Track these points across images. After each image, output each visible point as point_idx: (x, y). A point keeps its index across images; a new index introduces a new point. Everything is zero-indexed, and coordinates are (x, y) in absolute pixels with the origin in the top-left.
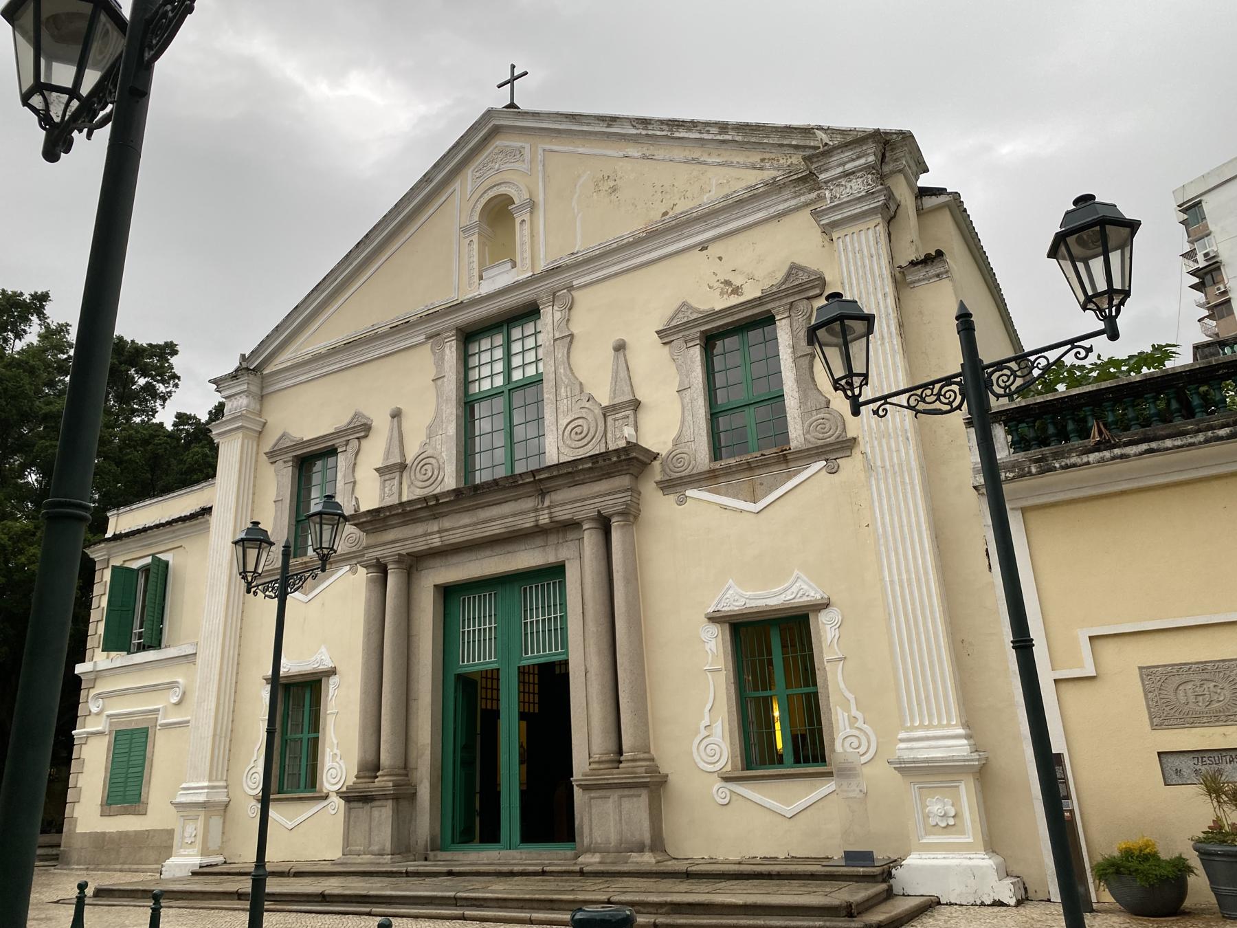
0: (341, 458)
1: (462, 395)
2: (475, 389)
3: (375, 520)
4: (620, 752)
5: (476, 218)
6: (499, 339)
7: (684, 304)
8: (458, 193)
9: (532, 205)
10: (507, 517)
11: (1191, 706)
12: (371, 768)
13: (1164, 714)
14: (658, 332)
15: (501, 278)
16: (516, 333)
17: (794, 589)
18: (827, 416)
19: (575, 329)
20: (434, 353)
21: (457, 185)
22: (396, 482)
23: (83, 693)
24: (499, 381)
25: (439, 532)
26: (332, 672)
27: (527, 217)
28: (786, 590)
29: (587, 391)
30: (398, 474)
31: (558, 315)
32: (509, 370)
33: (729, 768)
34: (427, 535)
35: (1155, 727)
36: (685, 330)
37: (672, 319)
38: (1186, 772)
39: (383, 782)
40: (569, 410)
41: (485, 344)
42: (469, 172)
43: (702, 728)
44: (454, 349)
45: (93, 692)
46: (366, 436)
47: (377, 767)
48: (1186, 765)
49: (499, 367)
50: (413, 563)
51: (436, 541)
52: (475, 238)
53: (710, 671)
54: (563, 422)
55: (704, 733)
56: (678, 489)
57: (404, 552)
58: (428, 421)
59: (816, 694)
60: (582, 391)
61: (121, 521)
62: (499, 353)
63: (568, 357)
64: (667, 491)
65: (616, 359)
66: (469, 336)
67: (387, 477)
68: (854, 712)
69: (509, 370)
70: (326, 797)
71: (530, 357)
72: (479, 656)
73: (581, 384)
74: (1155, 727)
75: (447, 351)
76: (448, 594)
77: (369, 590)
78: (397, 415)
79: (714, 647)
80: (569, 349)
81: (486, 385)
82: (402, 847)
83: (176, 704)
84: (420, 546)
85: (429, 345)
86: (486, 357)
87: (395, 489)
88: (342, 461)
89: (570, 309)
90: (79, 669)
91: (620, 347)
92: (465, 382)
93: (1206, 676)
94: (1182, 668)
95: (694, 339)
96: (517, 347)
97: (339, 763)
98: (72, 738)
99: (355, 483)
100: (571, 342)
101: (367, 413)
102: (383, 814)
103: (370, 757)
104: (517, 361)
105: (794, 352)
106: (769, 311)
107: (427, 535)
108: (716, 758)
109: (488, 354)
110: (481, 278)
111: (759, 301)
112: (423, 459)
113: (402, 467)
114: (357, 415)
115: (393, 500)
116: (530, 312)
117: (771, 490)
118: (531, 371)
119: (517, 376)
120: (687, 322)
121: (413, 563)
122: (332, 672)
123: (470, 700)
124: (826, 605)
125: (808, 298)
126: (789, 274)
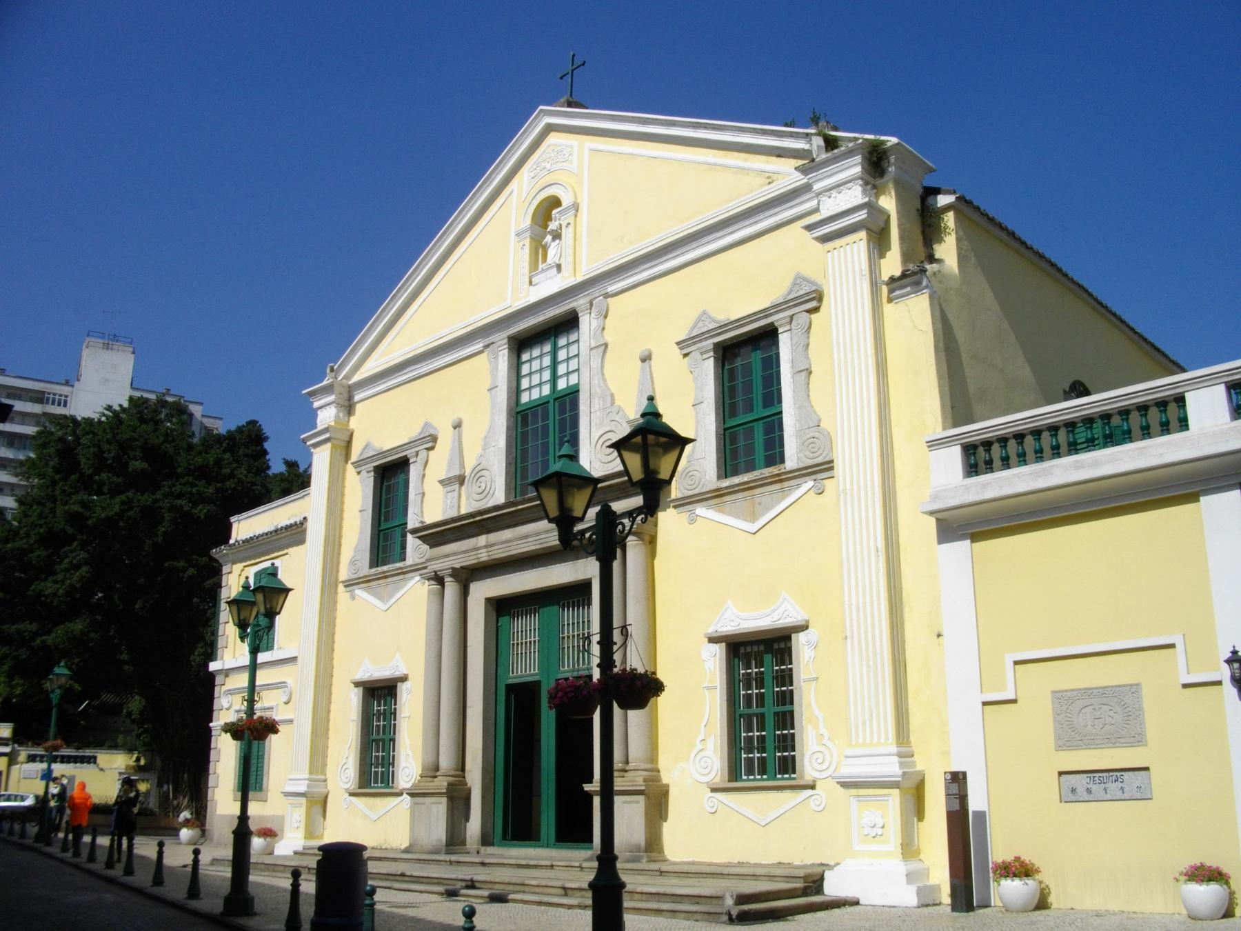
0: (412, 468)
1: (513, 405)
2: (525, 398)
3: (437, 535)
4: (627, 762)
5: (528, 222)
6: (547, 348)
7: (704, 313)
8: (514, 195)
9: (576, 207)
10: (541, 533)
11: (1089, 727)
12: (432, 770)
13: (1068, 738)
14: (678, 344)
15: (549, 285)
16: (562, 341)
17: (780, 611)
18: (816, 435)
19: (608, 337)
20: (490, 362)
21: (514, 185)
22: (456, 494)
23: (217, 689)
24: (546, 390)
25: (486, 547)
26: (404, 679)
27: (571, 220)
28: (774, 611)
29: (617, 403)
30: (456, 486)
31: (594, 323)
32: (554, 378)
33: (717, 780)
34: (483, 547)
35: (1059, 748)
36: (700, 341)
37: (694, 327)
38: (1081, 791)
39: (441, 783)
40: (602, 423)
41: (536, 352)
42: (525, 171)
43: (698, 741)
44: (506, 358)
45: (224, 688)
46: (432, 448)
47: (437, 768)
48: (1080, 782)
49: (547, 375)
50: (467, 576)
51: (484, 556)
52: (527, 242)
53: (708, 688)
54: (596, 435)
55: (699, 746)
56: (690, 507)
57: (457, 566)
58: (484, 434)
59: (792, 713)
60: (613, 403)
61: (245, 527)
62: (547, 361)
63: (602, 367)
64: (681, 509)
65: (643, 369)
66: (520, 344)
67: (449, 489)
68: (823, 730)
69: (554, 378)
70: (401, 794)
71: (573, 365)
72: (525, 668)
73: (612, 395)
74: (1059, 748)
75: (500, 360)
76: (501, 607)
77: (429, 602)
78: (458, 426)
79: (714, 660)
80: (603, 358)
81: (535, 394)
82: (455, 840)
83: (286, 703)
84: (470, 560)
85: (486, 353)
86: (536, 365)
87: (455, 500)
88: (414, 471)
89: (606, 317)
90: (213, 666)
91: (646, 359)
92: (516, 391)
93: (1105, 700)
94: (1087, 692)
95: (708, 351)
96: (562, 355)
97: (409, 764)
98: (209, 730)
99: (423, 494)
100: (605, 351)
101: (435, 424)
102: (439, 809)
103: (431, 759)
104: (562, 369)
105: (793, 367)
106: (772, 324)
107: (483, 547)
108: (706, 771)
109: (536, 359)
110: (531, 283)
111: (765, 313)
112: (479, 471)
113: (461, 480)
114: (427, 425)
115: (453, 514)
116: (569, 323)
117: (768, 509)
118: (573, 380)
119: (562, 384)
120: (703, 333)
121: (467, 576)
122: (404, 679)
123: (517, 706)
124: (803, 628)
125: (810, 311)
126: (794, 284)
